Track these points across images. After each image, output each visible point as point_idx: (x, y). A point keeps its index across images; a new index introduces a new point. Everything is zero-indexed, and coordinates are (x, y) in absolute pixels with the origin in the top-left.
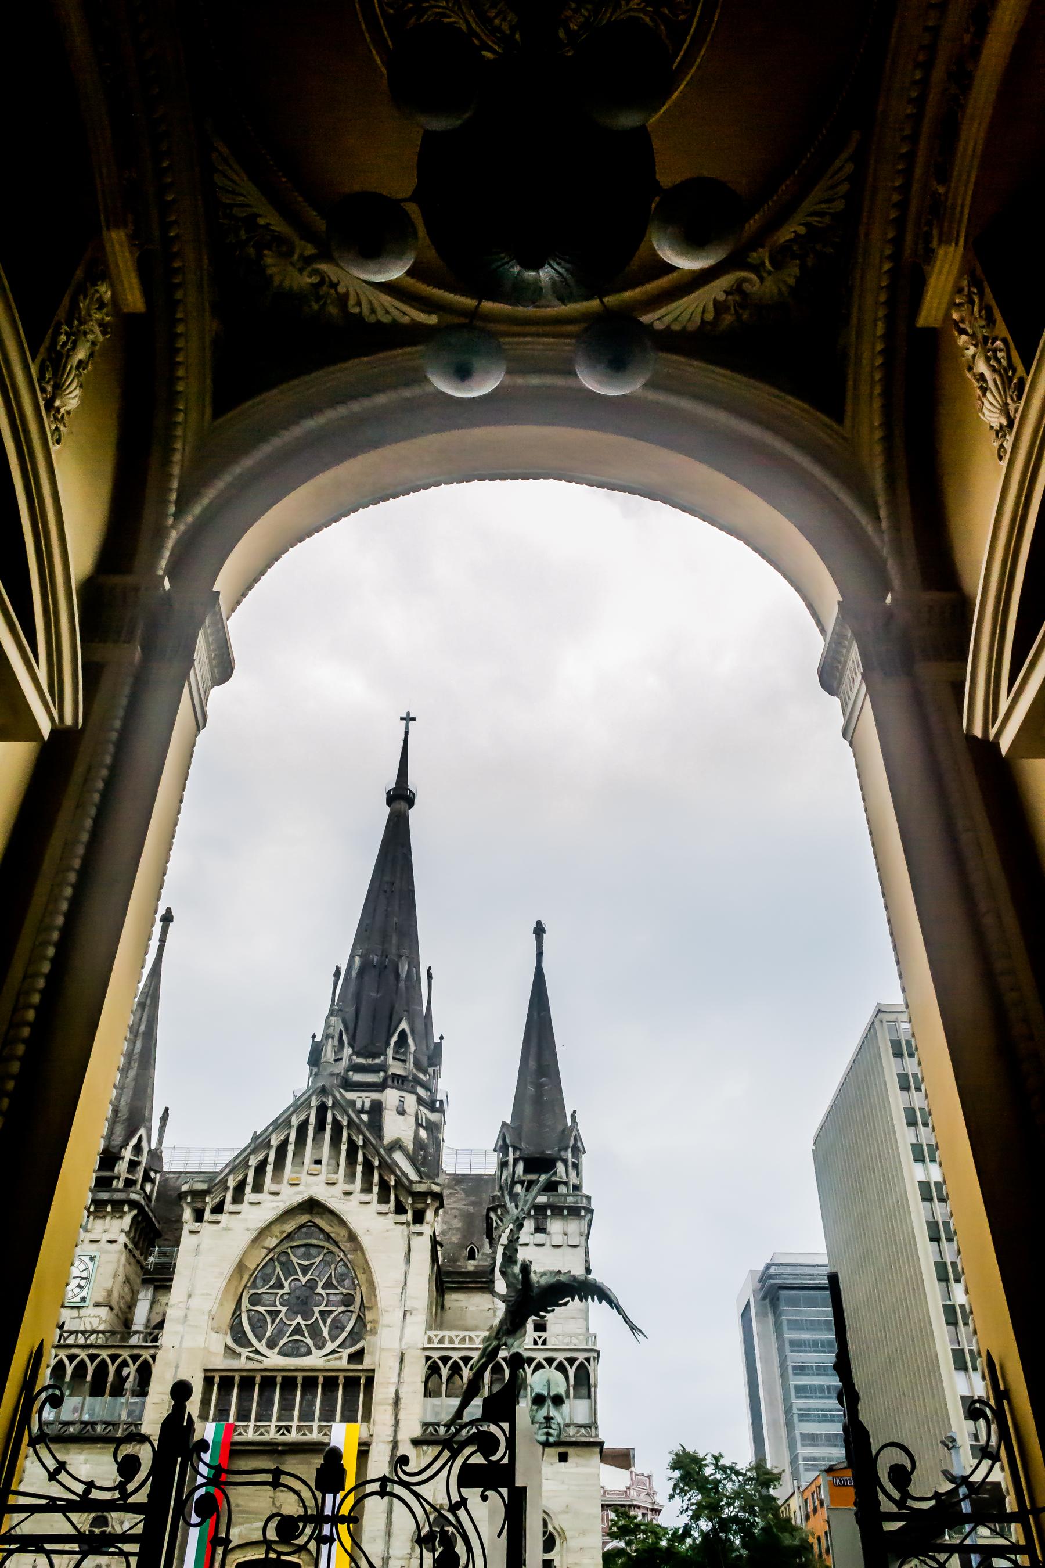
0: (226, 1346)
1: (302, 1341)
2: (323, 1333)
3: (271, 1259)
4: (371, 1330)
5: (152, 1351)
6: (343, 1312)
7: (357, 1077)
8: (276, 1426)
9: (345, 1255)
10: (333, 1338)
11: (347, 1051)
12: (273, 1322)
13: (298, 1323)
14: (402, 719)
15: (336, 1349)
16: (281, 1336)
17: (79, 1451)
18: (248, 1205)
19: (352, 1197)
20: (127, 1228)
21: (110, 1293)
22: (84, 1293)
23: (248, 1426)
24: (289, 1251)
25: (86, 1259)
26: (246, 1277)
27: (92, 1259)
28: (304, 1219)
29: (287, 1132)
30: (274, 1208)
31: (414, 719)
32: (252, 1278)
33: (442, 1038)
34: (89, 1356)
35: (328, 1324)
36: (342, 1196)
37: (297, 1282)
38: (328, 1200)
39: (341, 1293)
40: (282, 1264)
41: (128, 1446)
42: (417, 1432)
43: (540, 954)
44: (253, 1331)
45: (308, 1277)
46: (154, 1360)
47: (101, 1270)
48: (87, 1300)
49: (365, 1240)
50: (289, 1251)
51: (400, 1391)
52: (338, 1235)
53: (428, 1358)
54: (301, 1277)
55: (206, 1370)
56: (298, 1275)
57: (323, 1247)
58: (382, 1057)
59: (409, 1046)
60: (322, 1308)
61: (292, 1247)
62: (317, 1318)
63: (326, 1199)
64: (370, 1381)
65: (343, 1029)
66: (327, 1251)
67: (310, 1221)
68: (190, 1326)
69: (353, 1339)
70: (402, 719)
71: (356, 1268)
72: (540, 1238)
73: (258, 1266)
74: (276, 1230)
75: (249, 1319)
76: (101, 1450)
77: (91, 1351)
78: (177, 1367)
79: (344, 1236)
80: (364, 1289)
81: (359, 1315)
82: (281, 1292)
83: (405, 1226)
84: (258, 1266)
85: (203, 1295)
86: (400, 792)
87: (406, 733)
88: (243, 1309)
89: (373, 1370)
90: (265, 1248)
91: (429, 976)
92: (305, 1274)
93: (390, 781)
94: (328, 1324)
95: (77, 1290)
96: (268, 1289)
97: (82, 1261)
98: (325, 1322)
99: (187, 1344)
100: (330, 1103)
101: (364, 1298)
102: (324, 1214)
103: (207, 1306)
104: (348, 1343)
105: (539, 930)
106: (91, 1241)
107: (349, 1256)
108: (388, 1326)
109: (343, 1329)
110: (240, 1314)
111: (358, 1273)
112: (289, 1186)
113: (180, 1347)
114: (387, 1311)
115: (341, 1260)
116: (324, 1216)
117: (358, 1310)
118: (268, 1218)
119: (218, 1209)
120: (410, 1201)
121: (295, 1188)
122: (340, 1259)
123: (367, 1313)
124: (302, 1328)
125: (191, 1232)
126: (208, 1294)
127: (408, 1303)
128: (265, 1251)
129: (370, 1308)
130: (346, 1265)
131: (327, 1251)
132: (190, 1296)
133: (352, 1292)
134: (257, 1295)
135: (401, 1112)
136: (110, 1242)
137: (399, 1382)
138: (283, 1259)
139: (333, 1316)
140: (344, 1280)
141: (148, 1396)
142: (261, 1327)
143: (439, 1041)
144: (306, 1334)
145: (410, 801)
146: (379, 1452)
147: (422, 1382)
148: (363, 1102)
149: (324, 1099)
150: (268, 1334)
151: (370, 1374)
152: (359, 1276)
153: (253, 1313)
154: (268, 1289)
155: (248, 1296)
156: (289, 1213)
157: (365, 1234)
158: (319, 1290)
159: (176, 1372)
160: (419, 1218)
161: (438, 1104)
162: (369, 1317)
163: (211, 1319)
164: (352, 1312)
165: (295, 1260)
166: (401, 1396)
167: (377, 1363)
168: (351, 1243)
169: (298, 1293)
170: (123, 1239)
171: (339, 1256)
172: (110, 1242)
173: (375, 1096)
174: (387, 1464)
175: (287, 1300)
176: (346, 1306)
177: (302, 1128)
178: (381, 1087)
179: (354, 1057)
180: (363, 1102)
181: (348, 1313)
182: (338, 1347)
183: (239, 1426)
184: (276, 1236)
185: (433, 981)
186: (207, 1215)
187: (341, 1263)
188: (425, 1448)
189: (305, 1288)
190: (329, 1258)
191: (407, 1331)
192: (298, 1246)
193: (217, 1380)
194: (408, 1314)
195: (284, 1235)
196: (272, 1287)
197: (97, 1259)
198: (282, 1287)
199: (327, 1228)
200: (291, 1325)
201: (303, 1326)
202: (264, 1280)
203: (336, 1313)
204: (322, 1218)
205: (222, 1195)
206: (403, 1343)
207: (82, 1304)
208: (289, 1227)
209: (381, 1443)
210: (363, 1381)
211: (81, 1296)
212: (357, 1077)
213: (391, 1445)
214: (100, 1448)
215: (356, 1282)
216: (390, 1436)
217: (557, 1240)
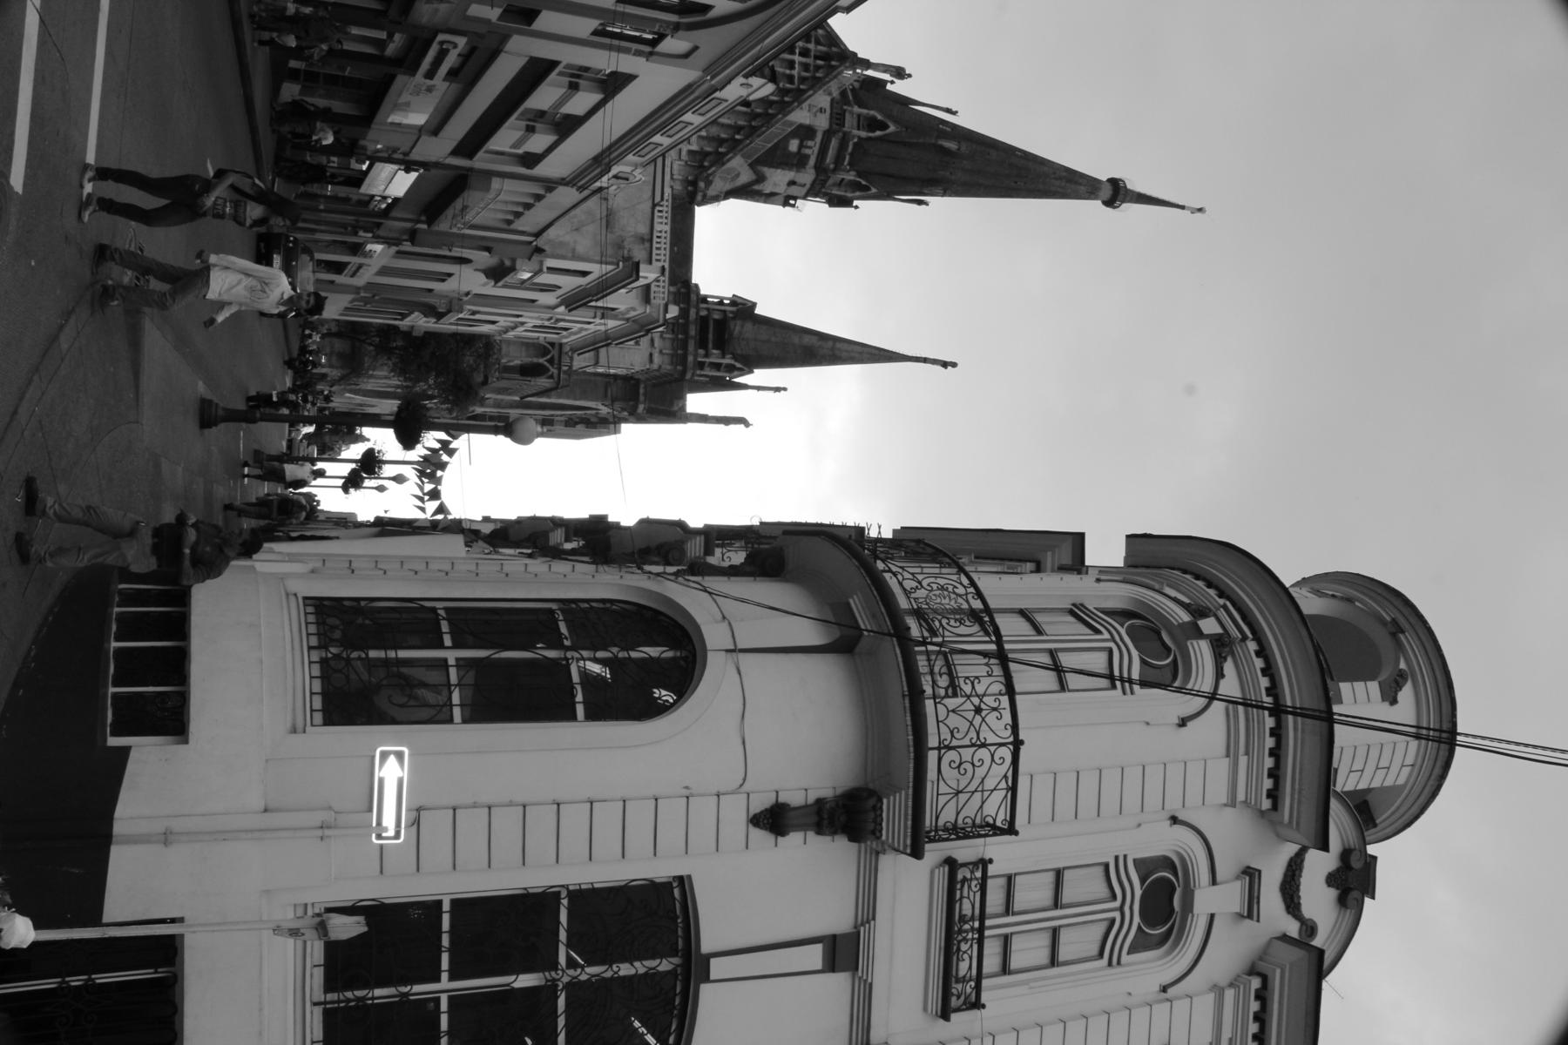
7: (834, 143)
11: (863, 134)
33: (856, 207)
58: (848, 167)
59: (854, 192)
65: (888, 131)
86: (1122, 192)
87: (1183, 207)
91: (920, 203)
93: (1135, 184)
135: (792, 183)
143: (854, 204)
148: (810, 147)
161: (792, 202)
173: (812, 161)
178: (820, 168)
179: (856, 140)
180: (810, 147)
185: (915, 206)
212: (834, 143)
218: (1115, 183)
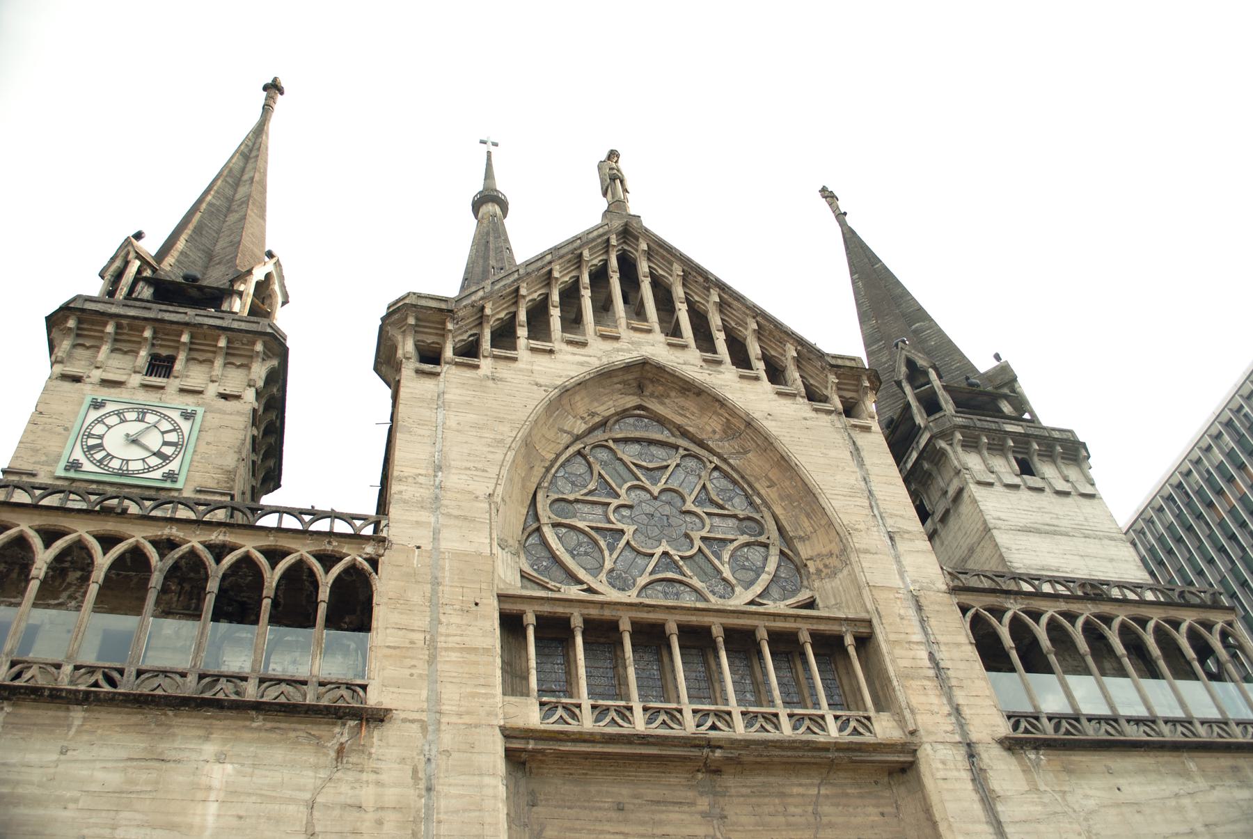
0: (524, 576)
1: (681, 582)
2: (719, 572)
3: (579, 453)
4: (819, 571)
5: (369, 549)
6: (748, 544)
8: (695, 712)
9: (725, 460)
10: (748, 585)
12: (612, 549)
13: (665, 554)
14: (483, 142)
15: (757, 600)
16: (635, 572)
17: (201, 732)
18: (529, 352)
19: (722, 368)
20: (260, 384)
21: (230, 474)
22: (174, 466)
23: (630, 709)
24: (611, 443)
25: (175, 415)
26: (539, 471)
27: (188, 416)
28: (631, 401)
29: (574, 274)
30: (582, 364)
31: (495, 144)
32: (550, 476)
34: (210, 547)
35: (726, 557)
36: (703, 364)
37: (638, 492)
38: (679, 366)
39: (735, 516)
40: (604, 464)
41: (337, 730)
42: (1004, 729)
43: (841, 216)
44: (573, 556)
45: (661, 485)
46: (377, 574)
47: (209, 437)
48: (181, 479)
49: (771, 427)
50: (611, 443)
51: (938, 656)
52: (702, 429)
53: (964, 609)
54: (647, 484)
55: (502, 597)
56: (638, 479)
57: (676, 447)
60: (704, 533)
61: (615, 441)
62: (700, 550)
63: (675, 365)
64: (865, 641)
66: (686, 453)
67: (640, 407)
68: (449, 515)
69: (784, 589)
70: (483, 142)
71: (752, 479)
72: (1031, 481)
73: (558, 456)
74: (582, 404)
75: (559, 538)
76: (263, 734)
77: (217, 537)
78: (436, 582)
79: (714, 432)
80: (779, 511)
81: (782, 552)
82: (615, 503)
83: (833, 417)
84: (558, 456)
85: (469, 469)
88: (544, 520)
89: (869, 622)
90: (568, 433)
92: (655, 482)
93: (478, 186)
94: (726, 557)
95: (154, 461)
96: (586, 494)
97: (165, 417)
98: (719, 558)
99: (452, 541)
100: (644, 246)
101: (785, 524)
102: (668, 396)
103: (483, 488)
104: (775, 592)
105: (828, 195)
106: (182, 391)
107: (731, 461)
108: (867, 551)
109: (758, 572)
110: (538, 529)
111: (757, 485)
112: (600, 339)
113: (436, 549)
114: (856, 530)
115: (716, 468)
116: (667, 401)
117: (777, 543)
118: (573, 374)
119: (470, 351)
120: (833, 379)
121: (616, 345)
122: (714, 465)
123: (800, 547)
124: (675, 562)
125: (419, 372)
126: (477, 469)
127: (889, 522)
128: (566, 439)
129: (801, 539)
130: (726, 475)
131: (686, 453)
132: (439, 468)
133: (757, 516)
134: (563, 504)
136: (225, 397)
137: (930, 643)
138: (603, 455)
139: (731, 547)
140: (731, 499)
141: (374, 633)
142: (586, 554)
144: (689, 573)
145: (504, 205)
146: (944, 763)
147: (971, 643)
149: (626, 247)
150: (608, 564)
151: (863, 630)
152: (762, 492)
153: (564, 530)
154: (586, 494)
155: (549, 502)
156: (606, 377)
157: (767, 418)
158: (689, 506)
159: (434, 592)
160: (850, 410)
162: (804, 551)
163: (494, 511)
164: (766, 546)
165: (625, 458)
166: (942, 664)
167: (870, 606)
168: (732, 443)
169: (648, 509)
170: (250, 395)
171: (711, 462)
172: (225, 397)
174: (970, 786)
175: (630, 517)
176: (751, 535)
177: (600, 277)
181: (762, 549)
182: (759, 596)
183: (608, 709)
184: (582, 418)
186: (448, 353)
187: (716, 474)
188: (1032, 755)
189: (658, 503)
190: (691, 463)
191: (907, 561)
192: (626, 441)
193: (530, 619)
194: (897, 538)
195: (597, 419)
196: (590, 493)
197: (199, 418)
198: (617, 496)
199: (678, 420)
200: (652, 555)
201: (677, 558)
202: (573, 483)
203: (736, 544)
204: (663, 403)
205: (472, 332)
206: (908, 580)
207: (168, 485)
208: (606, 408)
209: (940, 746)
210: (849, 640)
211: (166, 469)
213: (963, 750)
214: (258, 729)
215: (758, 501)
216: (953, 733)
217: (1062, 486)
218: (477, 205)
